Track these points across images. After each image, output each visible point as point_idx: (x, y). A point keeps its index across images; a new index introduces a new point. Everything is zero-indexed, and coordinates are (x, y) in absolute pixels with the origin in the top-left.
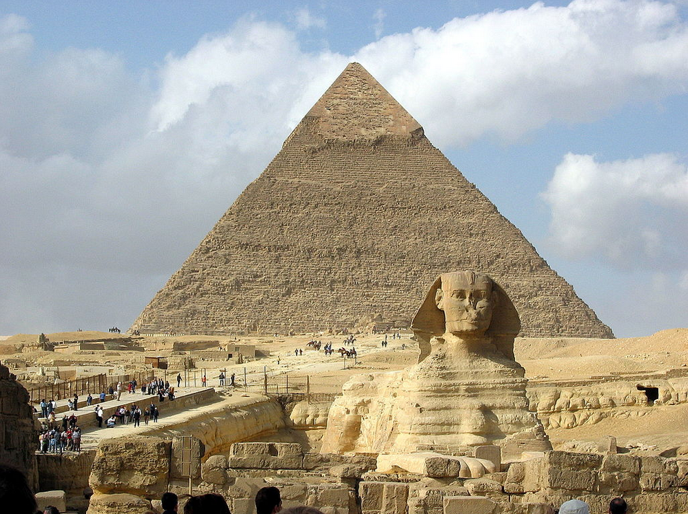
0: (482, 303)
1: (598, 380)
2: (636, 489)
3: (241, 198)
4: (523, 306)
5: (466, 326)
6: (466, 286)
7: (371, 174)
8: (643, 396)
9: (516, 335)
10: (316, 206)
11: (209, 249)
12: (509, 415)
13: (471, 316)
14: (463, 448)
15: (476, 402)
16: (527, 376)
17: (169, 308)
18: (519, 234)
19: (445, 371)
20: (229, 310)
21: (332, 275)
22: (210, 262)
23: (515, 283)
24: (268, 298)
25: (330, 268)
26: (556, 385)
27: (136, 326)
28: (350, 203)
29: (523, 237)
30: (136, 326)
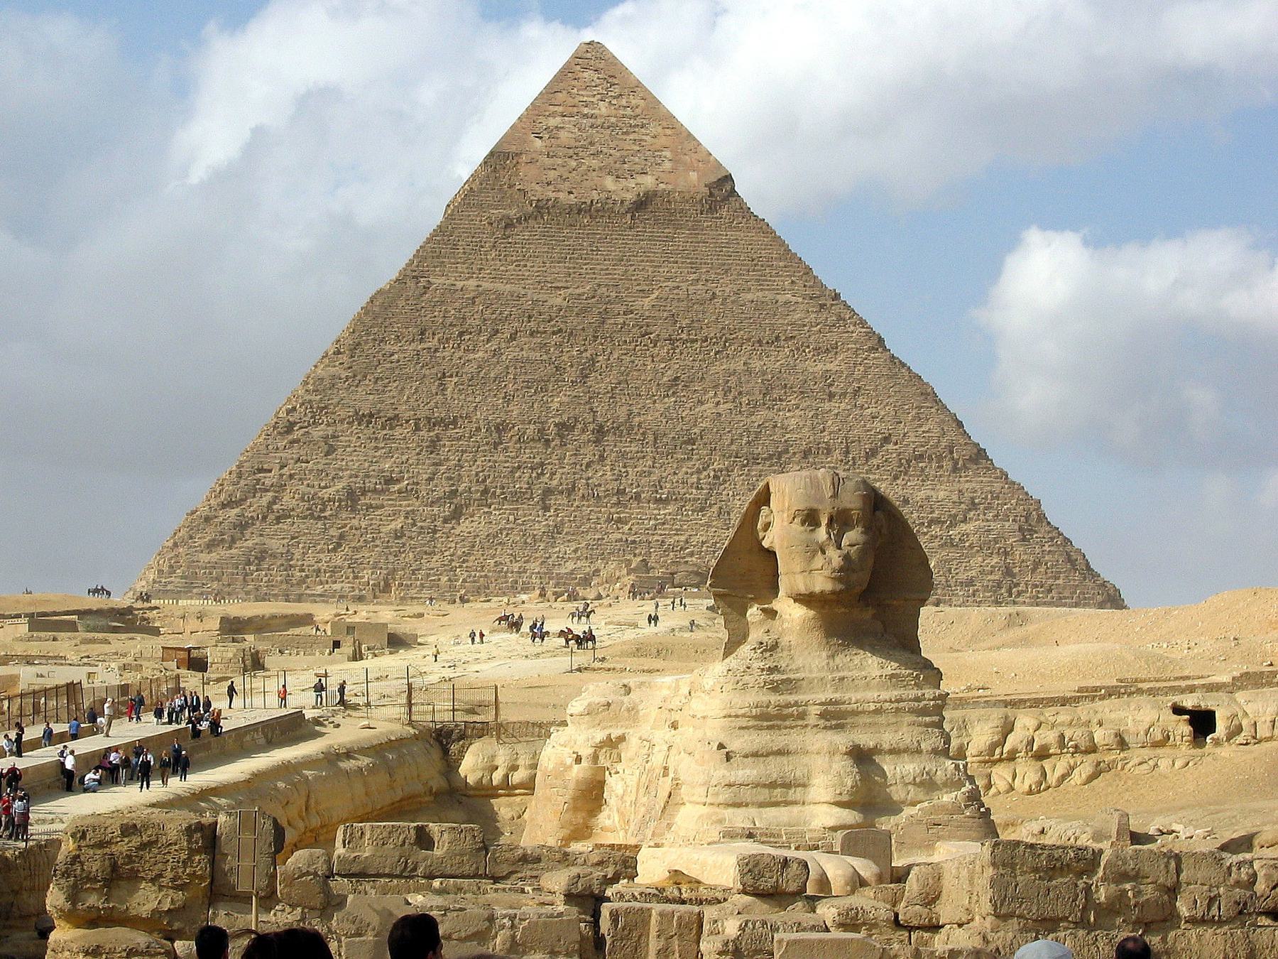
0: (853, 536)
1: (1091, 694)
2: (1169, 918)
3: (359, 320)
4: (936, 544)
5: (821, 583)
6: (821, 500)
7: (626, 271)
8: (1183, 728)
9: (923, 602)
10: (513, 337)
11: (296, 423)
12: (909, 767)
13: (830, 562)
14: (815, 835)
15: (842, 740)
16: (945, 686)
17: (211, 546)
18: (929, 395)
19: (777, 677)
20: (335, 550)
21: (545, 479)
22: (294, 452)
23: (922, 494)
24: (414, 525)
25: (542, 464)
26: (1006, 704)
27: (144, 583)
28: (583, 329)
29: (937, 401)
30: (144, 583)
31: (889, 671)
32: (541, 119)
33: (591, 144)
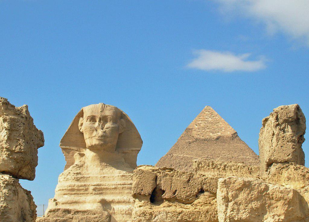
5: (95, 142)
10: (190, 166)
15: (99, 198)
31: (121, 174)
32: (197, 122)
33: (208, 126)
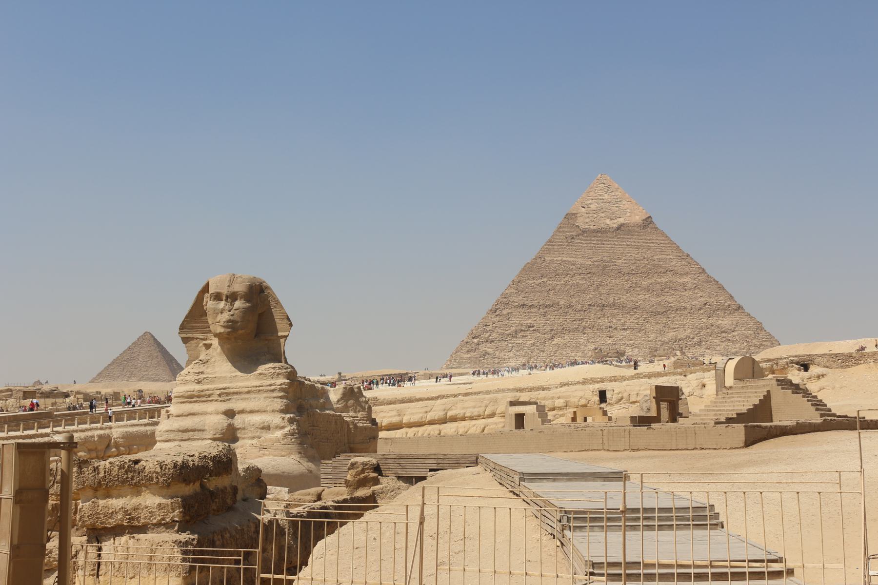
5: (220, 330)
12: (257, 419)
17: (468, 351)
18: (722, 288)
22: (497, 319)
